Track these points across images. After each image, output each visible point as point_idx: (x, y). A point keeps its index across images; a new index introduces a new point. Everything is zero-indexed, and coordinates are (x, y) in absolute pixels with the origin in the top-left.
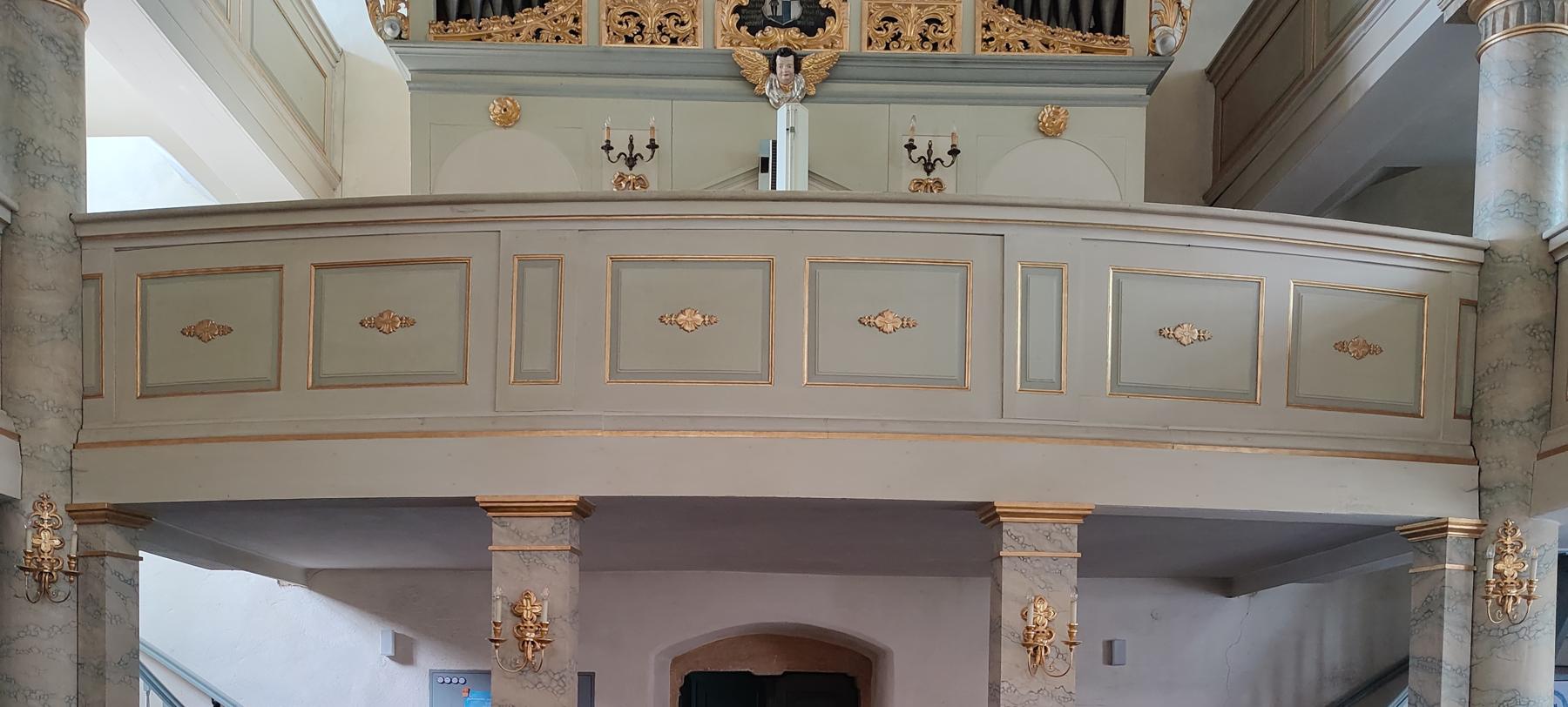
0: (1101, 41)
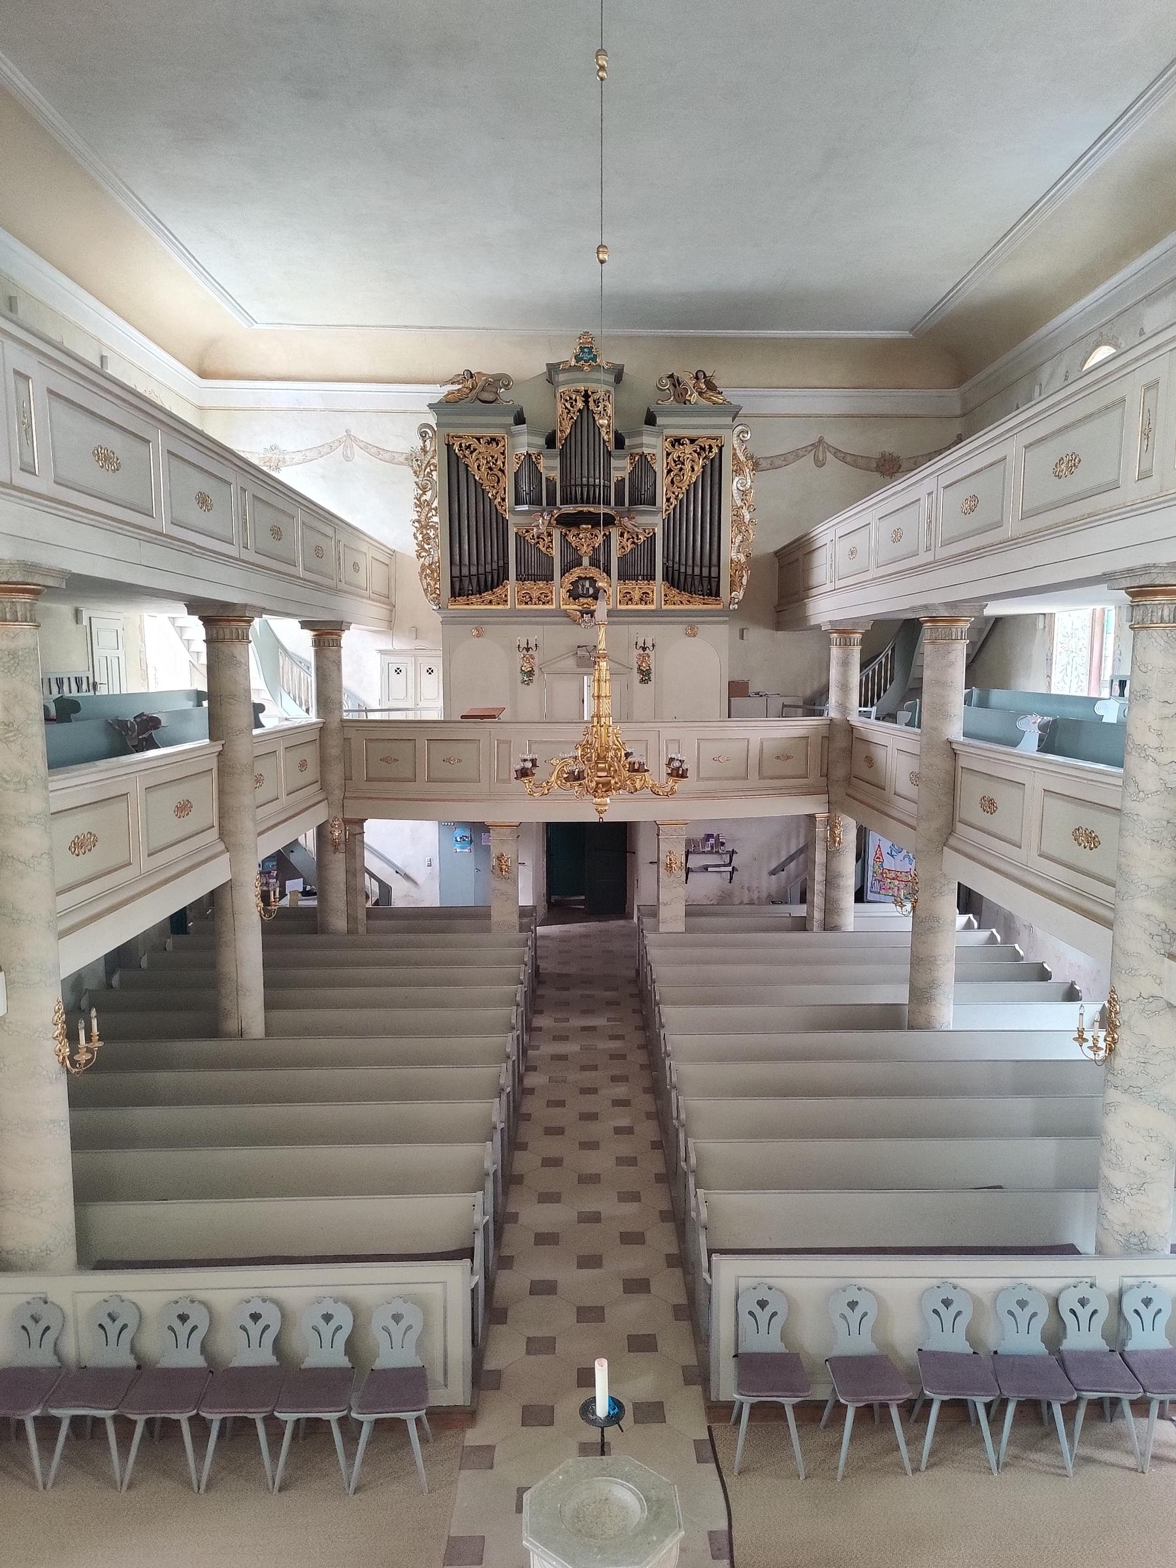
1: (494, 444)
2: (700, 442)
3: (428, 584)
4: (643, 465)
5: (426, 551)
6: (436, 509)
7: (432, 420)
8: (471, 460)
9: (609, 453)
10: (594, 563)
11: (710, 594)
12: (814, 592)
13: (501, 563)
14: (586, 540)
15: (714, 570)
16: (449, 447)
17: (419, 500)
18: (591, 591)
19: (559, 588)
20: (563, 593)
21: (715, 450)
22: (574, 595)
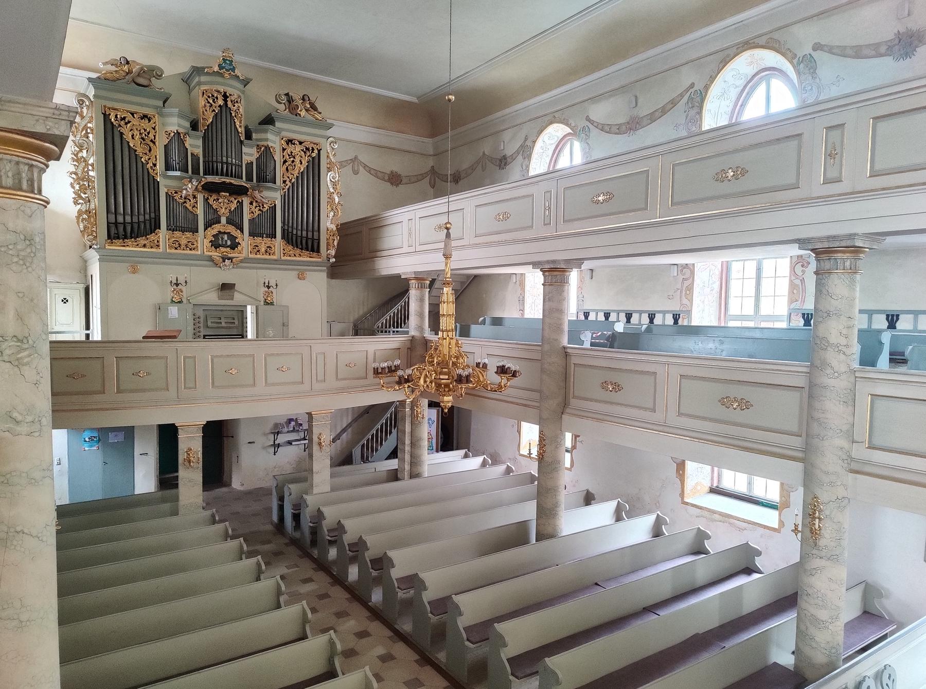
0: (315, 254)
1: (147, 121)
2: (307, 144)
3: (85, 227)
4: (266, 153)
5: (83, 199)
6: (92, 165)
7: (91, 92)
8: (126, 130)
9: (242, 142)
10: (229, 222)
11: (313, 251)
12: (379, 254)
13: (153, 215)
14: (224, 205)
15: (316, 234)
16: (106, 117)
17: (76, 155)
18: (229, 243)
19: (203, 240)
20: (207, 243)
21: (316, 151)
22: (215, 245)
